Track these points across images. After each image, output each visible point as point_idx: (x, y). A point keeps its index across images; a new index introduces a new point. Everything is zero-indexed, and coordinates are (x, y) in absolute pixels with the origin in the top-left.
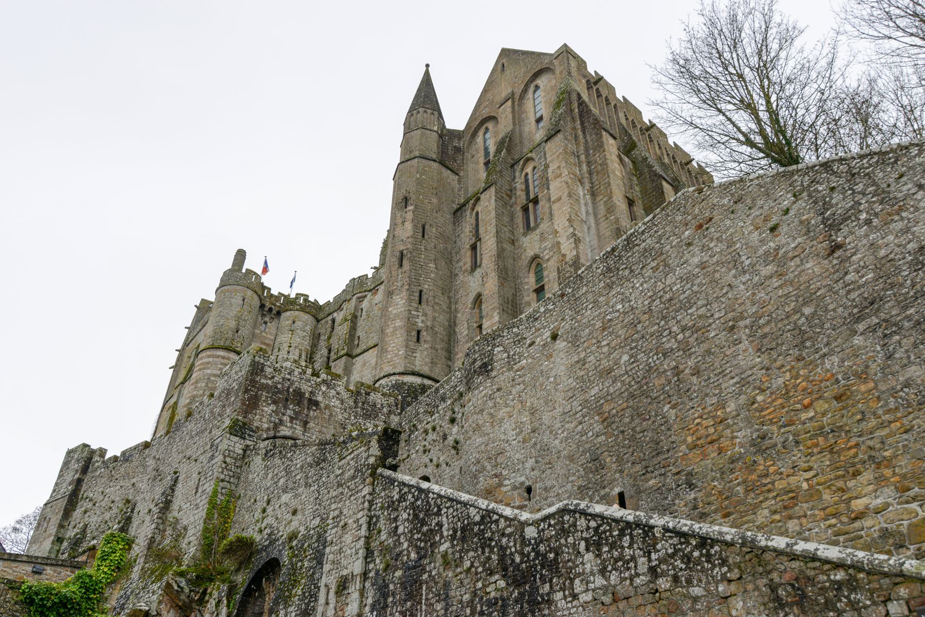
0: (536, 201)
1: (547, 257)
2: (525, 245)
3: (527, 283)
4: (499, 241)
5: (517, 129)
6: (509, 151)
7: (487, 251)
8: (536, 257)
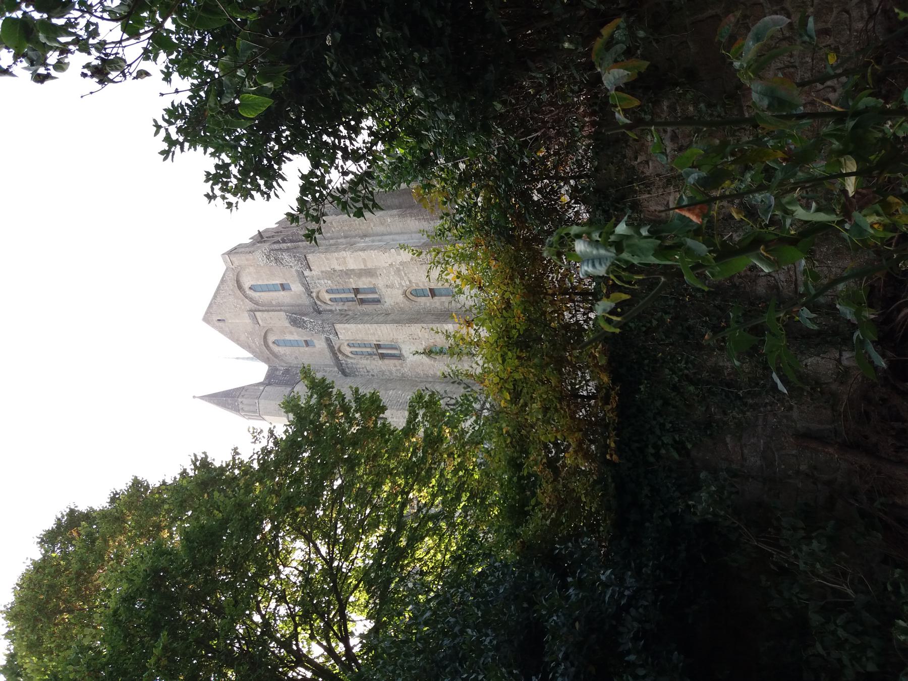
0: (357, 291)
1: (408, 283)
2: (393, 304)
3: (425, 304)
4: (386, 322)
5: (286, 308)
6: (305, 315)
7: (391, 335)
8: (405, 293)
